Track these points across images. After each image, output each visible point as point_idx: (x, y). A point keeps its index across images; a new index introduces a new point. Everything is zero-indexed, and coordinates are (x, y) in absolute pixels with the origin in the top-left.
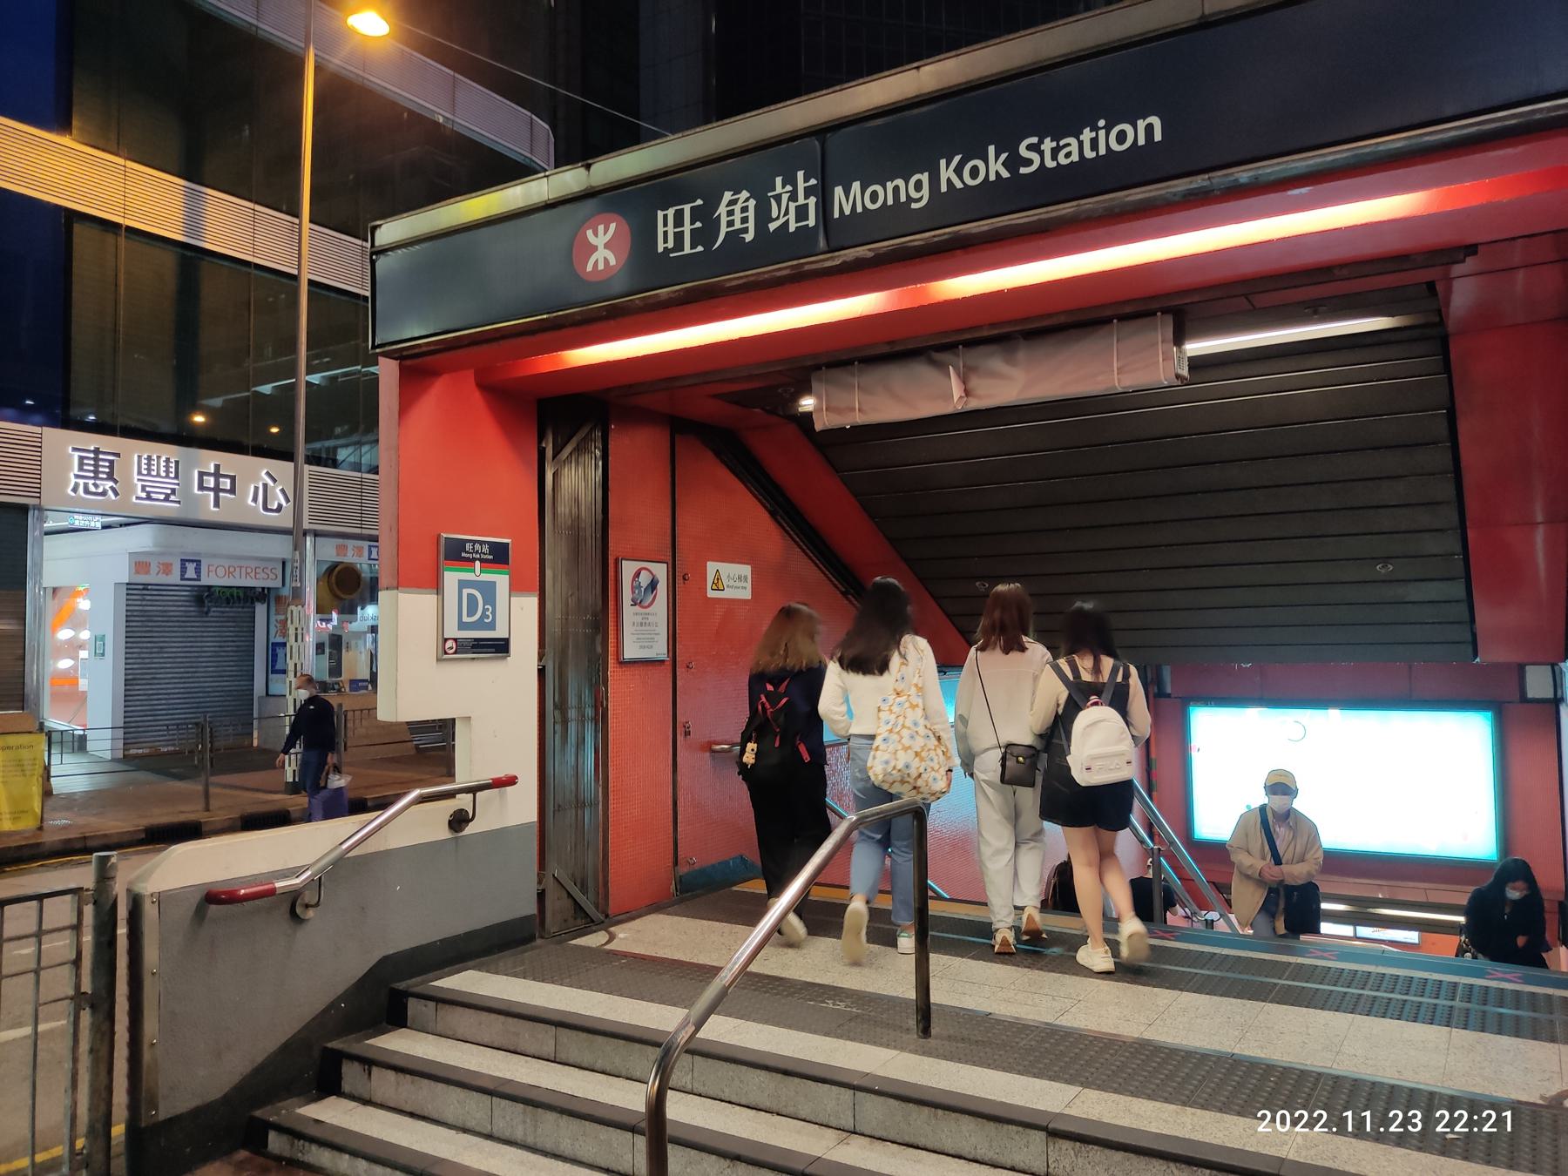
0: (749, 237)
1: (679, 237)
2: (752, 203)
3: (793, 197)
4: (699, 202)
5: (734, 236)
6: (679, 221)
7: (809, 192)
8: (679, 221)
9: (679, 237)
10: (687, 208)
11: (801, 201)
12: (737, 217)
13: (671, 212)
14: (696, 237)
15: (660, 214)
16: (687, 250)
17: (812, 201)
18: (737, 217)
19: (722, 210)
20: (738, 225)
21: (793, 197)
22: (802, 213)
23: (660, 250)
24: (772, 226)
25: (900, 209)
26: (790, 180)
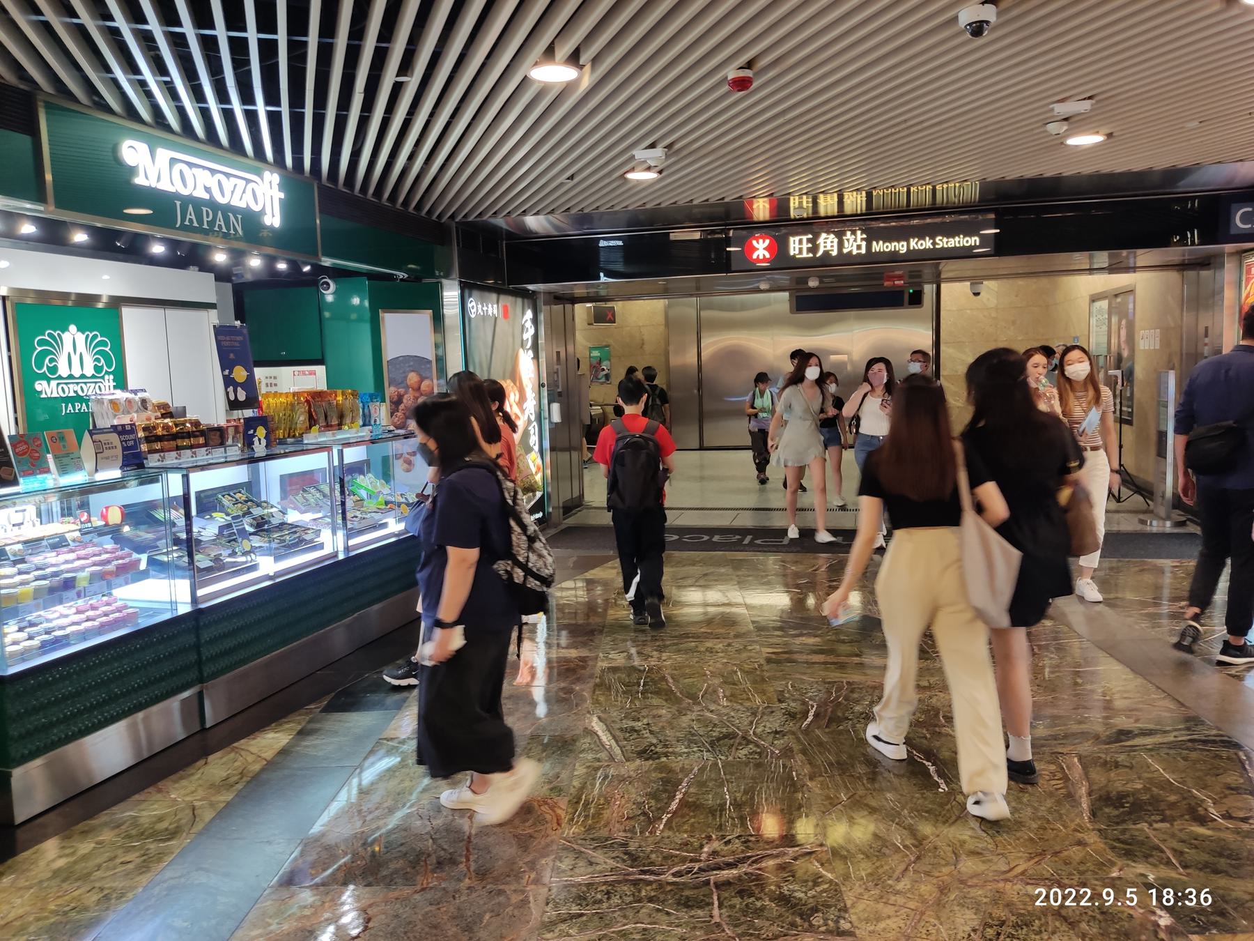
0: (834, 253)
1: (801, 250)
2: (836, 240)
3: (855, 240)
4: (810, 236)
5: (826, 253)
6: (801, 242)
7: (862, 239)
8: (801, 242)
9: (801, 250)
10: (804, 238)
11: (859, 242)
12: (829, 245)
13: (797, 239)
14: (809, 250)
15: (792, 239)
16: (805, 255)
17: (864, 244)
18: (829, 245)
19: (821, 241)
20: (829, 248)
21: (855, 240)
22: (859, 247)
23: (792, 253)
24: (845, 251)
25: (895, 253)
26: (854, 233)
